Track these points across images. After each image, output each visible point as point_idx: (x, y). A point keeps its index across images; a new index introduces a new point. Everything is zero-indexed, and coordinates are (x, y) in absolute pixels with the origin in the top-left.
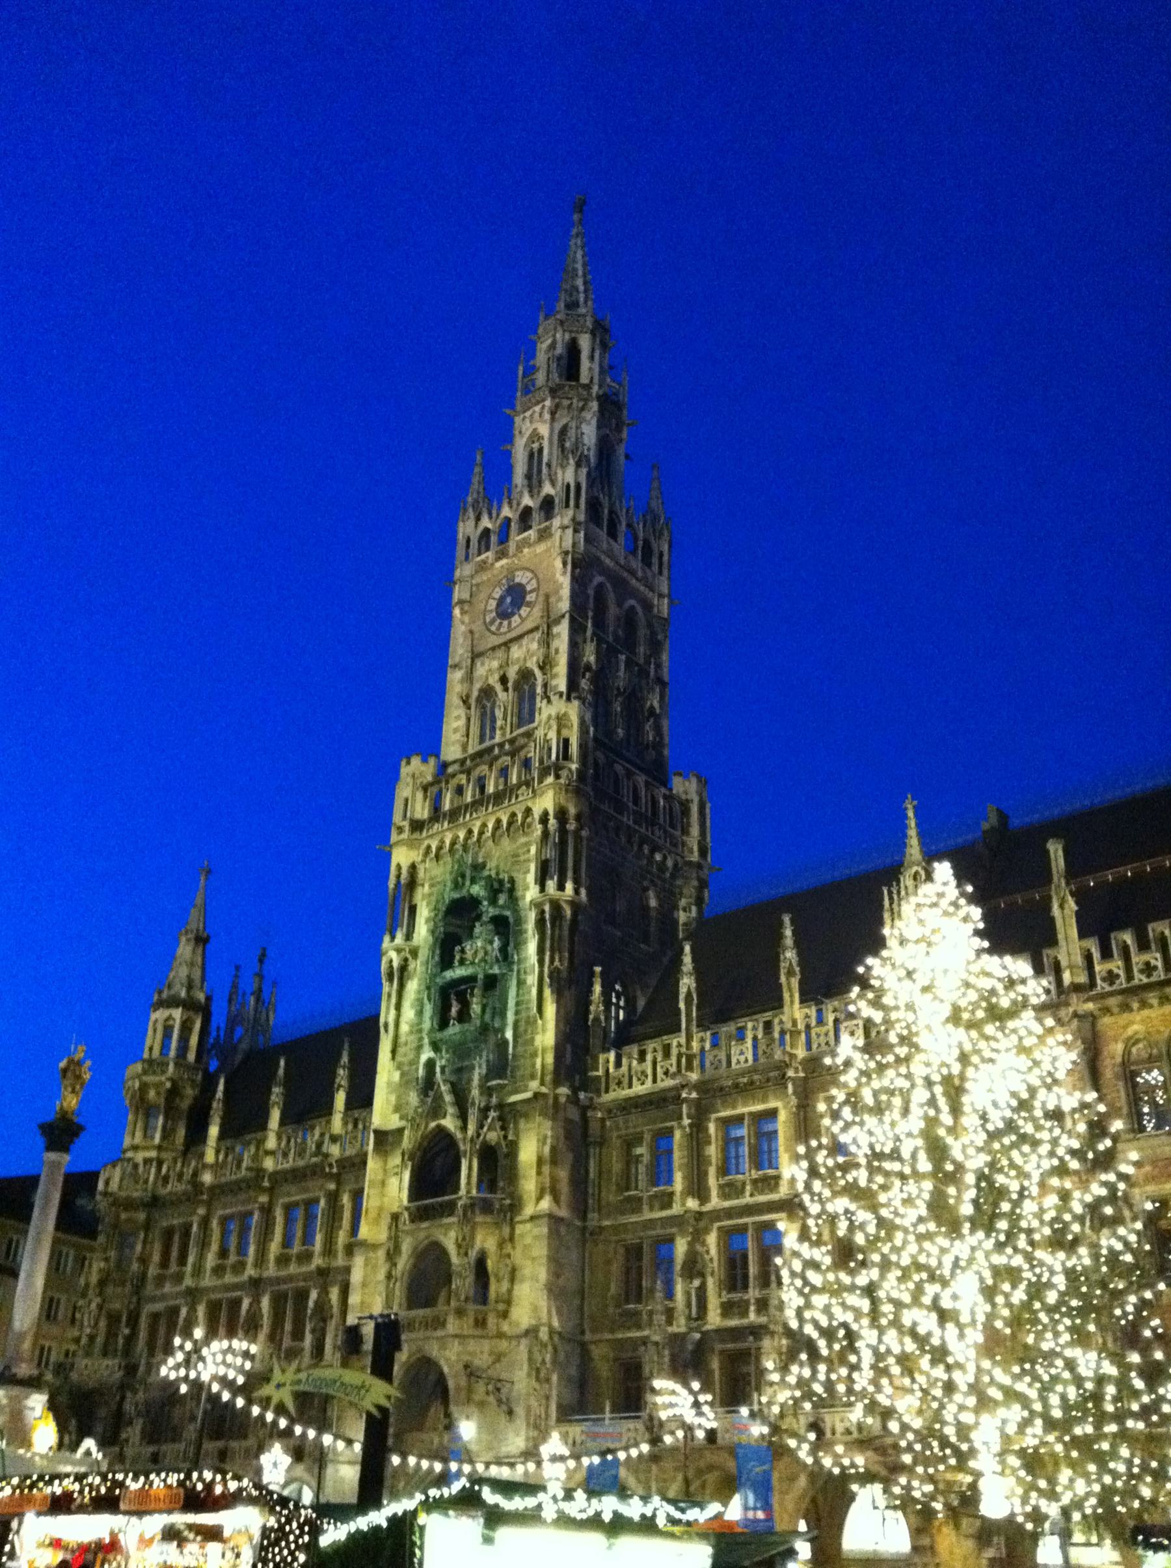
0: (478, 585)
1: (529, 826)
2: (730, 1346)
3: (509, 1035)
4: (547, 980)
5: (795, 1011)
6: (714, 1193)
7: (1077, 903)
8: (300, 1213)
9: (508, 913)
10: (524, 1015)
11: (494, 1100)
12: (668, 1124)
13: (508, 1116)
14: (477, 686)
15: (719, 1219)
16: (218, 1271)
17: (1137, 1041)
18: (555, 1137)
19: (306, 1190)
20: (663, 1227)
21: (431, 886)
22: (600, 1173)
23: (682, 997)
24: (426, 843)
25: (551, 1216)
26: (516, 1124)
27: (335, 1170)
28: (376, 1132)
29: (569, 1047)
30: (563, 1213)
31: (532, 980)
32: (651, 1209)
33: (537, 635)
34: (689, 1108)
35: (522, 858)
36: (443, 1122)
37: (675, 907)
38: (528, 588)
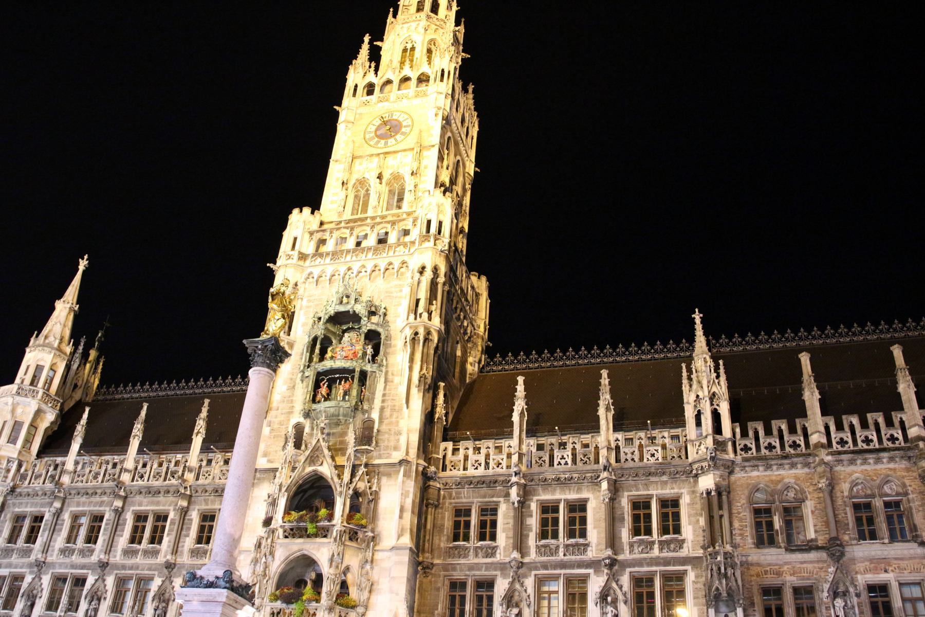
0: (360, 114)
1: (402, 274)
3: (375, 415)
5: (606, 435)
6: (533, 551)
7: (820, 393)
9: (380, 330)
10: (389, 403)
11: (364, 460)
12: (495, 499)
13: (372, 471)
15: (536, 568)
16: (63, 551)
17: (857, 484)
18: (415, 495)
19: (158, 503)
20: (486, 569)
21: (309, 301)
24: (309, 270)
25: (411, 549)
27: (188, 493)
32: (477, 556)
33: (410, 154)
35: (395, 295)
36: (320, 469)
37: (466, 361)
38: (404, 124)
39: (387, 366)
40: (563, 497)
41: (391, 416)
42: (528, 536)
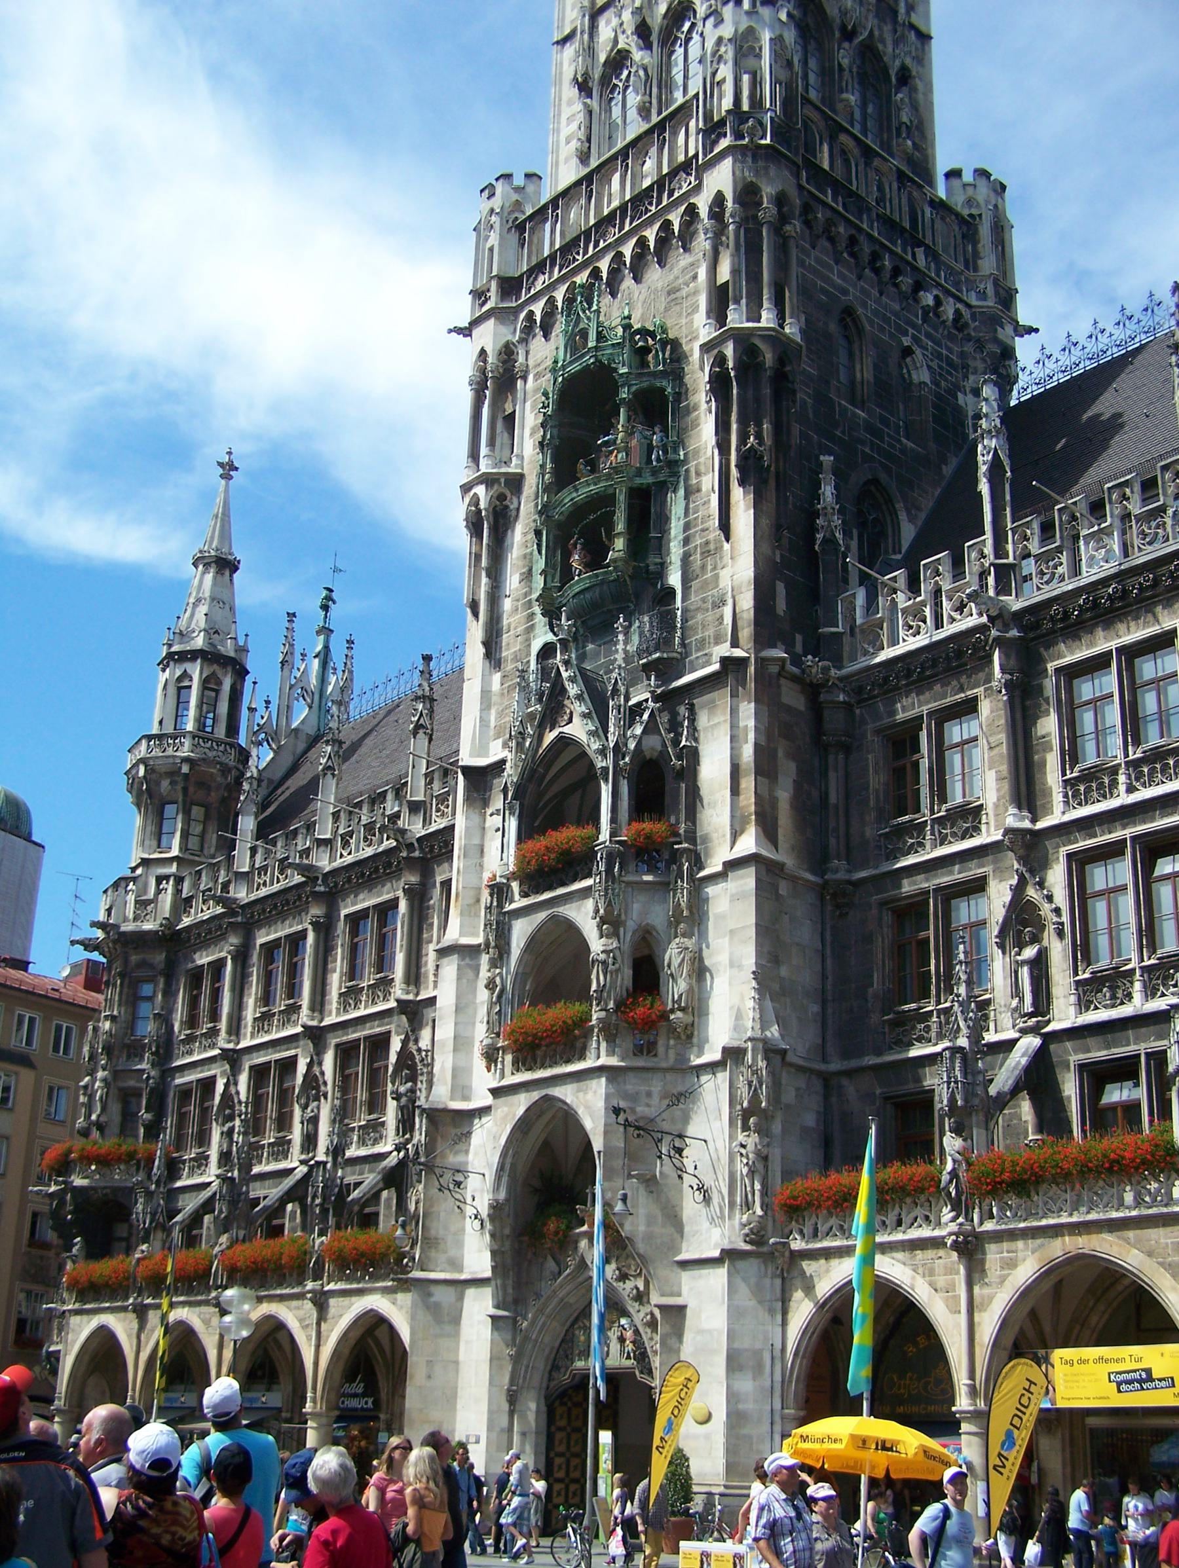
2: (1100, 1054)
3: (674, 579)
4: (734, 472)
6: (1057, 798)
8: (371, 925)
13: (677, 704)
14: (602, 58)
21: (537, 376)
22: (847, 797)
23: (983, 468)
26: (693, 720)
28: (468, 771)
29: (781, 588)
30: (784, 856)
31: (709, 482)
34: (1005, 655)
35: (684, 293)
36: (566, 729)
39: (685, 461)
40: (1113, 644)
41: (703, 567)
42: (1043, 764)
